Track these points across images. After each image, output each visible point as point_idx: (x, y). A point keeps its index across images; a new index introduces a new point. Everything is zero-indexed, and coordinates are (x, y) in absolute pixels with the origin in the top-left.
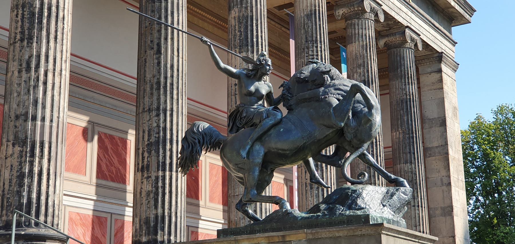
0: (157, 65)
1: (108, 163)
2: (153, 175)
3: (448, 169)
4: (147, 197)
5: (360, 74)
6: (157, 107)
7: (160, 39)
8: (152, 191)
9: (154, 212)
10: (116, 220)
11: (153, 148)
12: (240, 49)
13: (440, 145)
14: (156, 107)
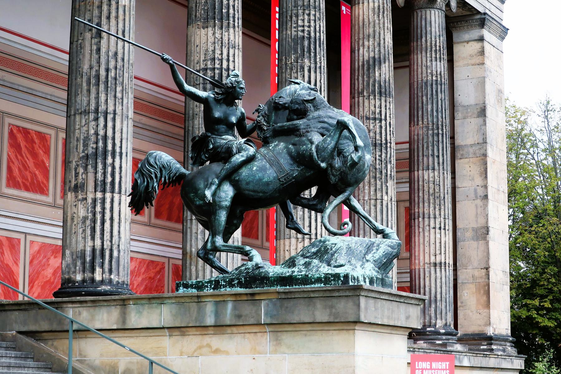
0: (96, 52)
1: (21, 167)
2: (90, 196)
3: (485, 176)
4: (82, 225)
5: (369, 48)
6: (95, 109)
7: (100, 17)
8: (88, 216)
9: (90, 243)
10: (32, 242)
11: (89, 162)
12: (204, 23)
13: (476, 143)
14: (93, 108)
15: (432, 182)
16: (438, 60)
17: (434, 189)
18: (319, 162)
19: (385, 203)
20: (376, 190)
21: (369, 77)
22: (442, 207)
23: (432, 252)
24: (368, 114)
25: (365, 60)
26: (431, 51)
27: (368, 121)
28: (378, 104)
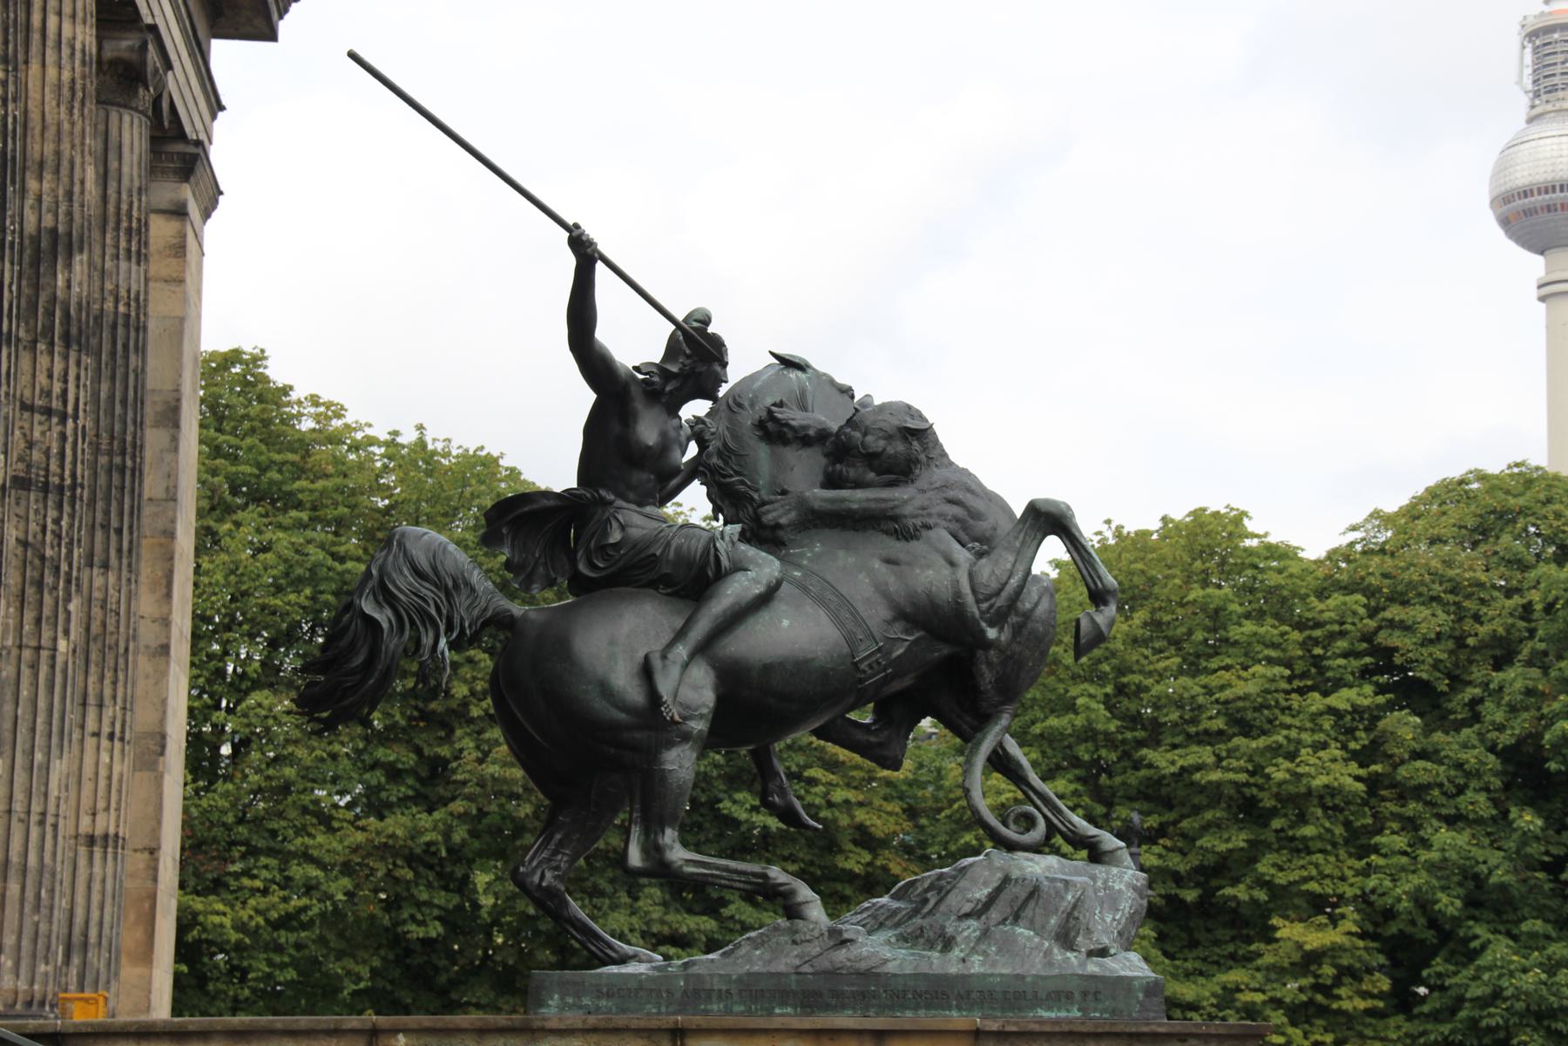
3: (164, 591)
5: (39, 199)
15: (99, 603)
16: (134, 259)
17: (104, 625)
18: (984, 624)
19: (60, 660)
20: (38, 621)
21: (37, 287)
22: (121, 676)
23: (86, 802)
24: (27, 393)
25: (26, 233)
26: (117, 228)
27: (26, 415)
28: (58, 368)
